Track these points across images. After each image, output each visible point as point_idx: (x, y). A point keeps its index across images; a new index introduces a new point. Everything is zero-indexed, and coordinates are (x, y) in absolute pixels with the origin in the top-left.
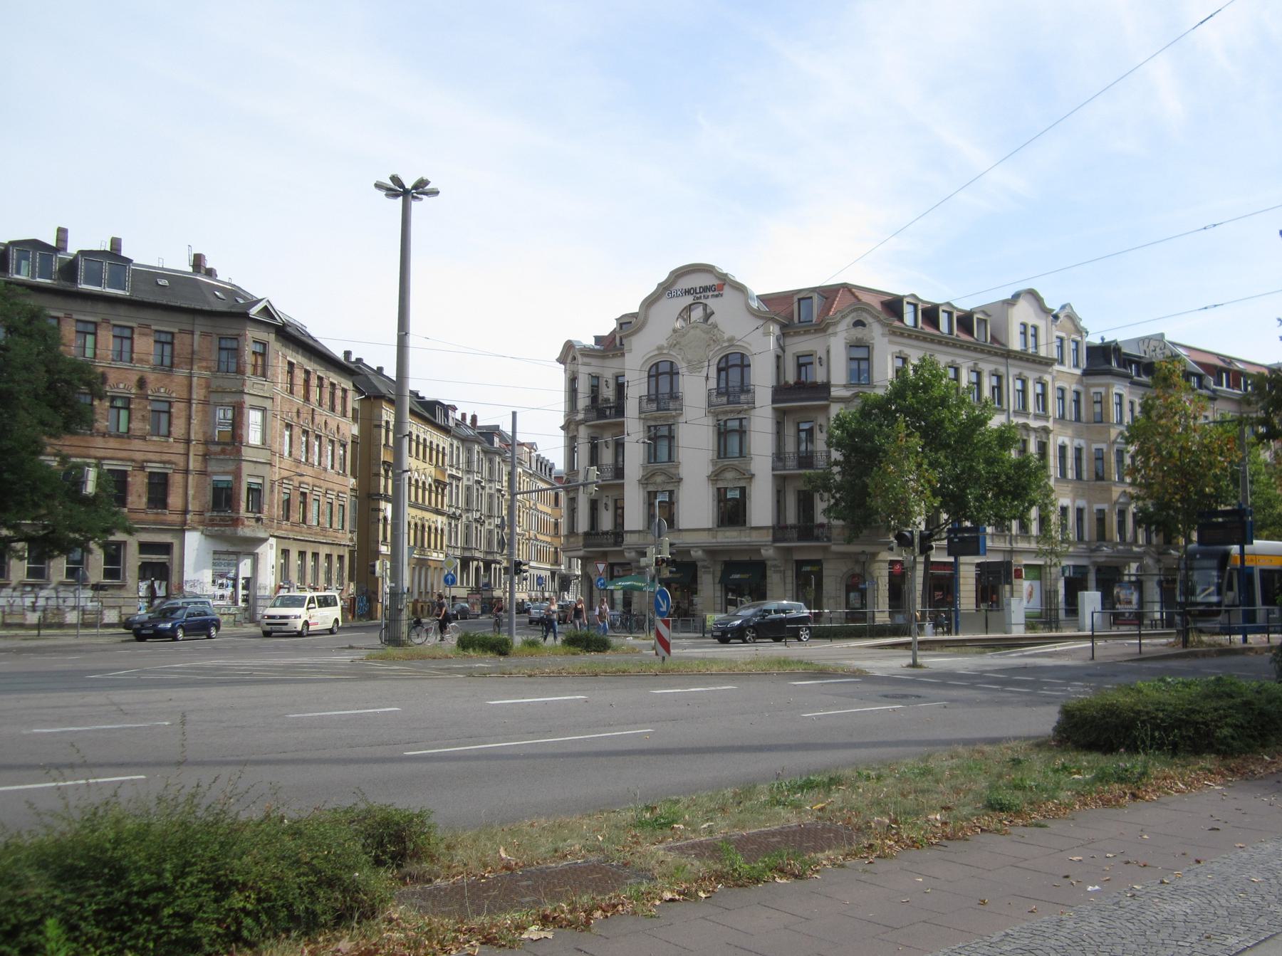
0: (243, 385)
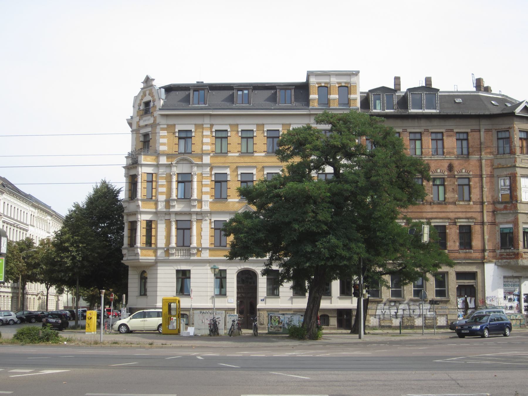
0: (515, 161)
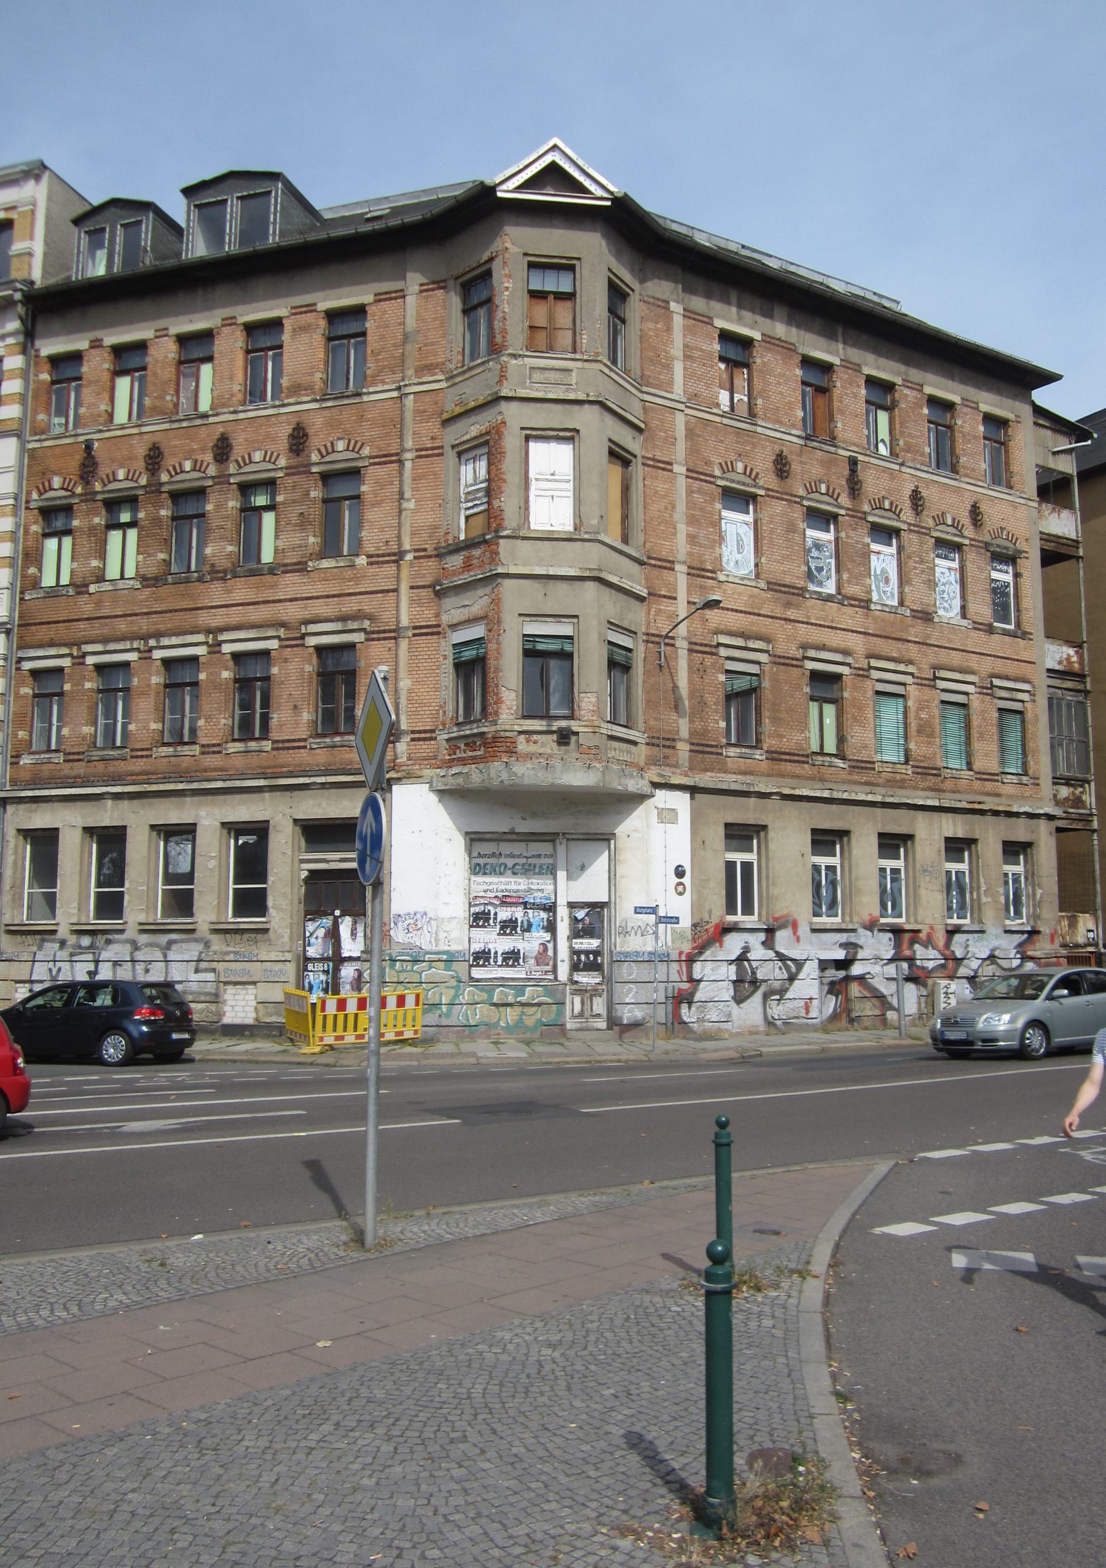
0: (502, 377)
